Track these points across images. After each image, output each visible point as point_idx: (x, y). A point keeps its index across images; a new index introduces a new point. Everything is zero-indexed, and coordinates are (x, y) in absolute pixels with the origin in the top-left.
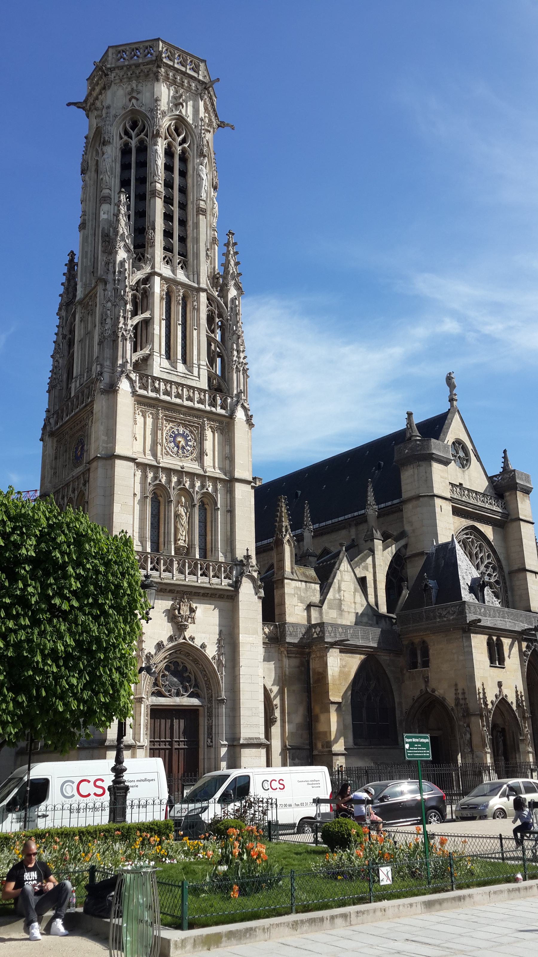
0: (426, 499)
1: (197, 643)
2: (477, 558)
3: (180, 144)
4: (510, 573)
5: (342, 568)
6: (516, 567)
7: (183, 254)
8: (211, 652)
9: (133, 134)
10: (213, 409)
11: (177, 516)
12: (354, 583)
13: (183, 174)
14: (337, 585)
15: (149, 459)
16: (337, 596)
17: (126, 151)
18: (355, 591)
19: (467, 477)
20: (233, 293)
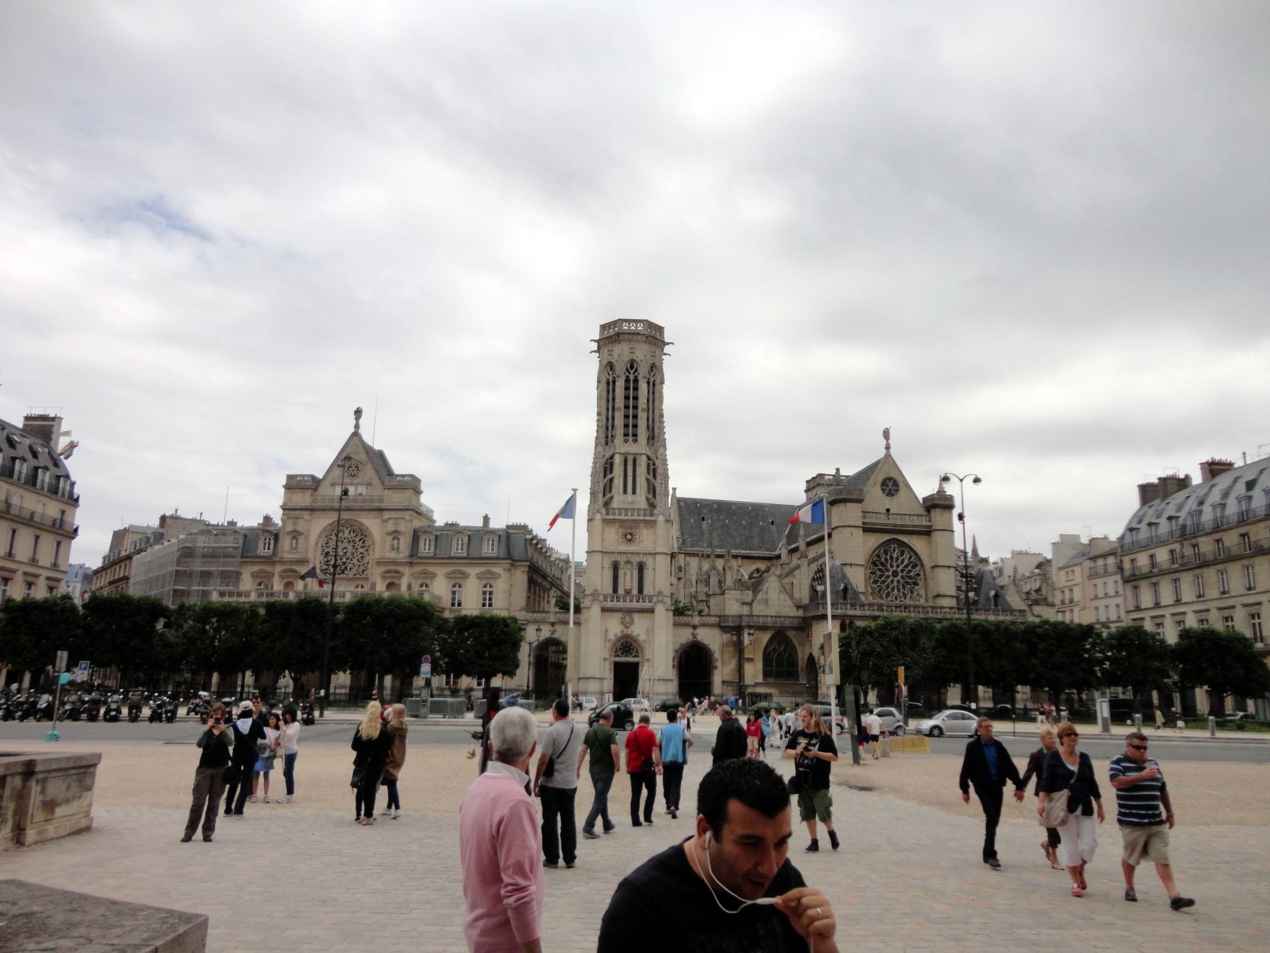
0: (840, 528)
1: (635, 634)
2: (897, 559)
3: (634, 373)
4: (933, 567)
5: (770, 579)
6: (934, 564)
7: (635, 435)
8: (642, 637)
9: (610, 373)
10: (646, 518)
11: (625, 574)
12: (779, 588)
13: (636, 389)
14: (765, 590)
15: (612, 549)
16: (765, 597)
17: (608, 383)
18: (780, 592)
19: (895, 503)
20: (661, 450)
